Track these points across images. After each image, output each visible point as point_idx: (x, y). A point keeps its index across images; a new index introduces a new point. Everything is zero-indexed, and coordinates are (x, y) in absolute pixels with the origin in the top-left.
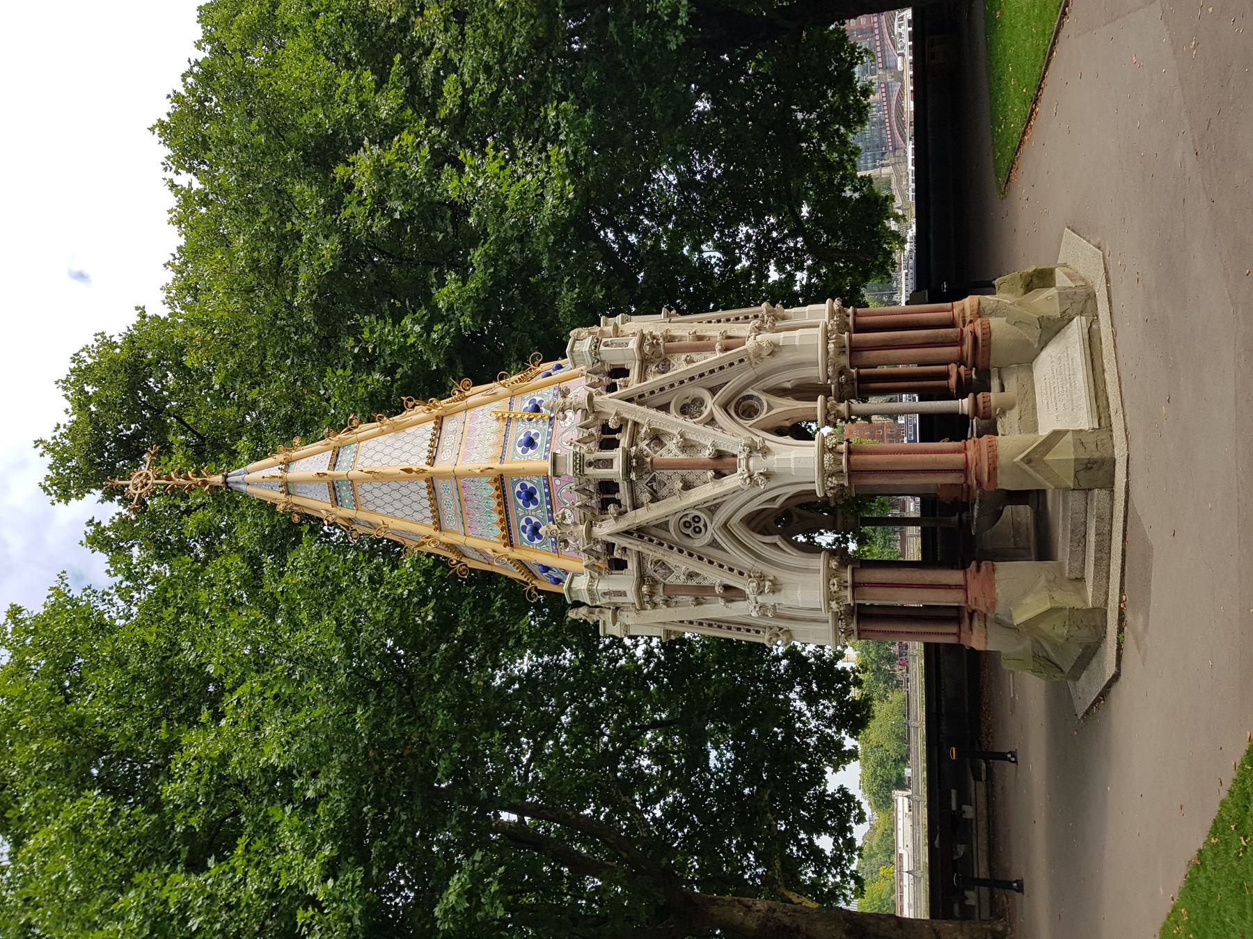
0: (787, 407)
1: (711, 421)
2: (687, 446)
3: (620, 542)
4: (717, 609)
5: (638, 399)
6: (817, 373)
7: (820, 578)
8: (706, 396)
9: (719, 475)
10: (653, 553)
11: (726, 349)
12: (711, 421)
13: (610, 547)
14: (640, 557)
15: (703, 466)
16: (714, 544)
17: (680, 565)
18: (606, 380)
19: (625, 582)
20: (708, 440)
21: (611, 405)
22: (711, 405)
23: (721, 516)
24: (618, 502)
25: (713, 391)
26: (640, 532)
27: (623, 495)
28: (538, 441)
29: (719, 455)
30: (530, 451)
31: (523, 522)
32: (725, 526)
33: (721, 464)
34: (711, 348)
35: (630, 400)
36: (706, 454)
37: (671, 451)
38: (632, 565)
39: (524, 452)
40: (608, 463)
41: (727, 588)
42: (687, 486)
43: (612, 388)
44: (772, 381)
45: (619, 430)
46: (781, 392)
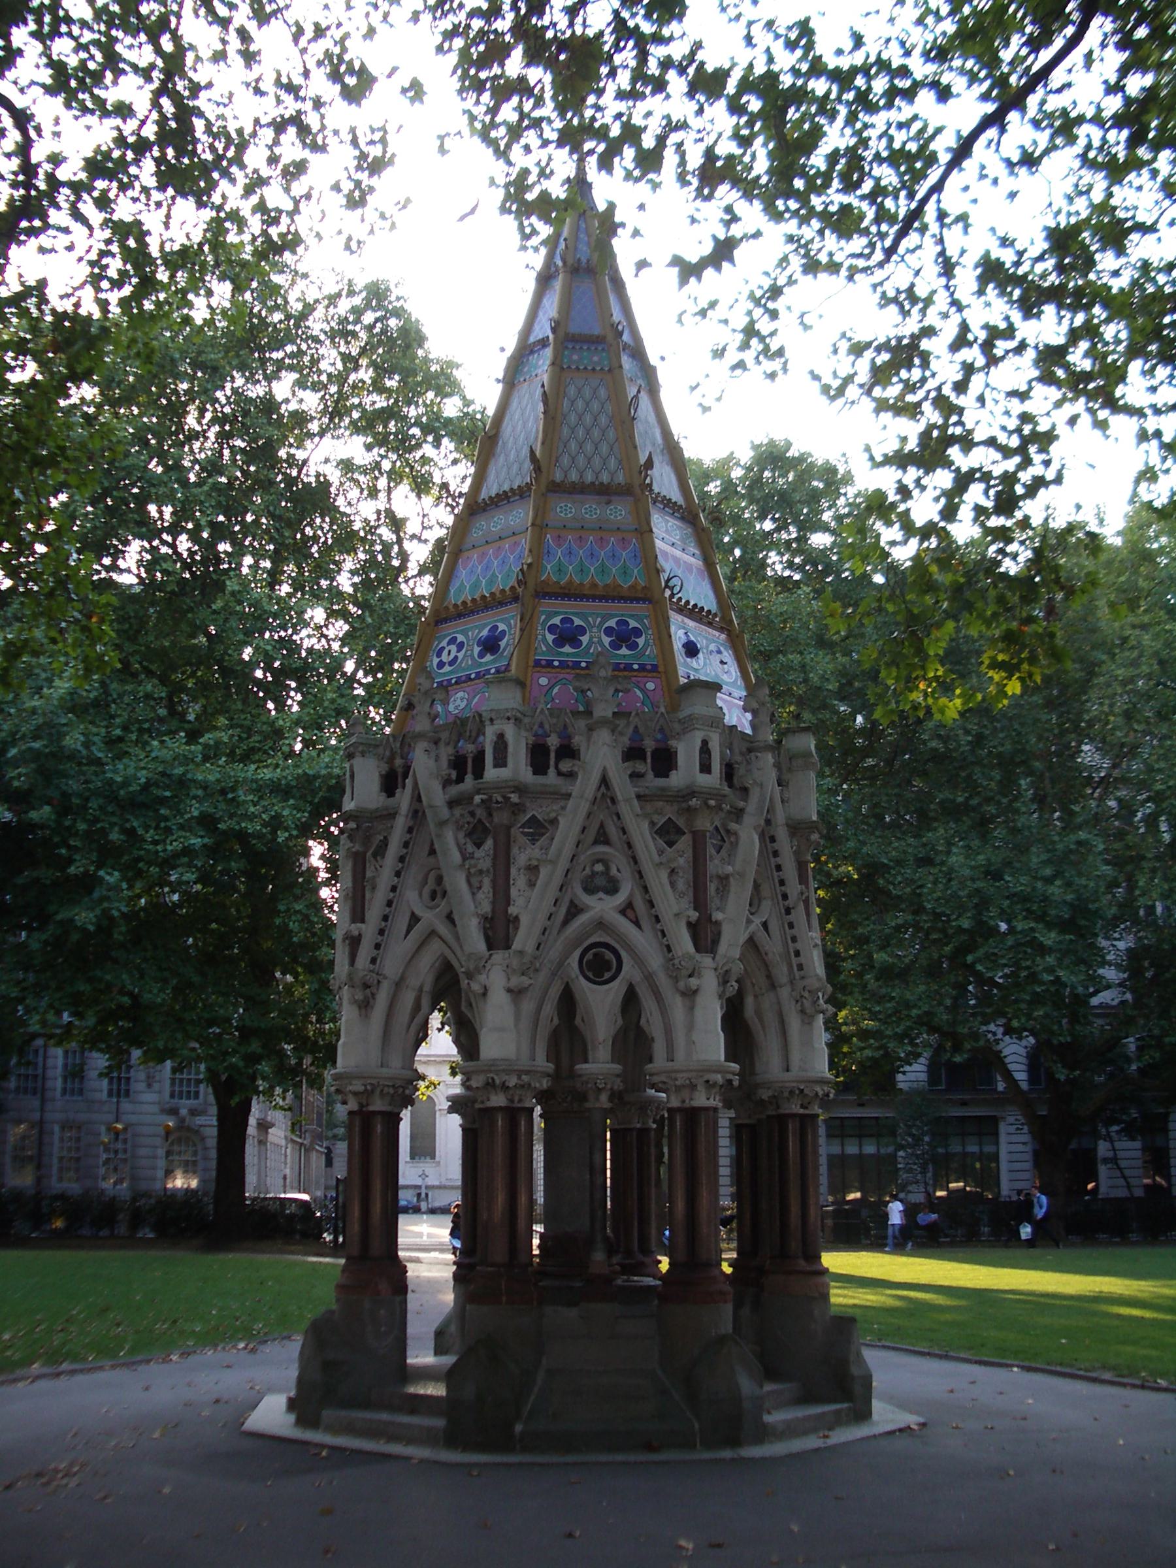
8: (620, 898)
11: (693, 927)
12: (574, 910)
15: (502, 895)
16: (415, 919)
18: (649, 745)
20: (530, 906)
22: (603, 906)
23: (443, 929)
24: (460, 779)
25: (627, 909)
26: (417, 814)
28: (567, 649)
30: (550, 638)
31: (460, 638)
32: (433, 933)
33: (499, 931)
34: (699, 902)
35: (604, 781)
37: (523, 855)
39: (552, 629)
43: (633, 753)
44: (644, 993)
45: (560, 774)
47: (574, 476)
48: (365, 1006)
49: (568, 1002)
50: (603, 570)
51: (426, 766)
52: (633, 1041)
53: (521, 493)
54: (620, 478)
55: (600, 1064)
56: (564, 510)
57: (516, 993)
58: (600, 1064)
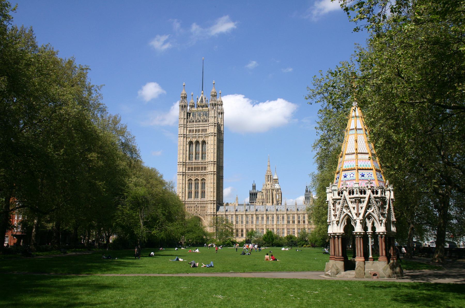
0: (369, 225)
1: (366, 212)
2: (362, 208)
3: (343, 195)
4: (333, 212)
5: (369, 198)
6: (377, 231)
7: (339, 232)
8: (372, 210)
9: (356, 214)
10: (341, 201)
13: (342, 193)
14: (340, 199)
15: (358, 210)
16: (344, 212)
17: (338, 206)
19: (337, 196)
21: (369, 192)
22: (370, 211)
25: (373, 212)
27: (352, 196)
29: (360, 214)
32: (347, 214)
36: (360, 212)
38: (339, 197)
40: (357, 194)
41: (336, 215)
42: (354, 208)
43: (373, 192)
44: (375, 221)
46: (373, 224)
47: (361, 152)
48: (338, 225)
49: (366, 223)
50: (366, 166)
51: (346, 193)
52: (374, 228)
53: (354, 154)
54: (367, 152)
55: (370, 230)
56: (360, 156)
57: (361, 223)
58: (370, 230)
